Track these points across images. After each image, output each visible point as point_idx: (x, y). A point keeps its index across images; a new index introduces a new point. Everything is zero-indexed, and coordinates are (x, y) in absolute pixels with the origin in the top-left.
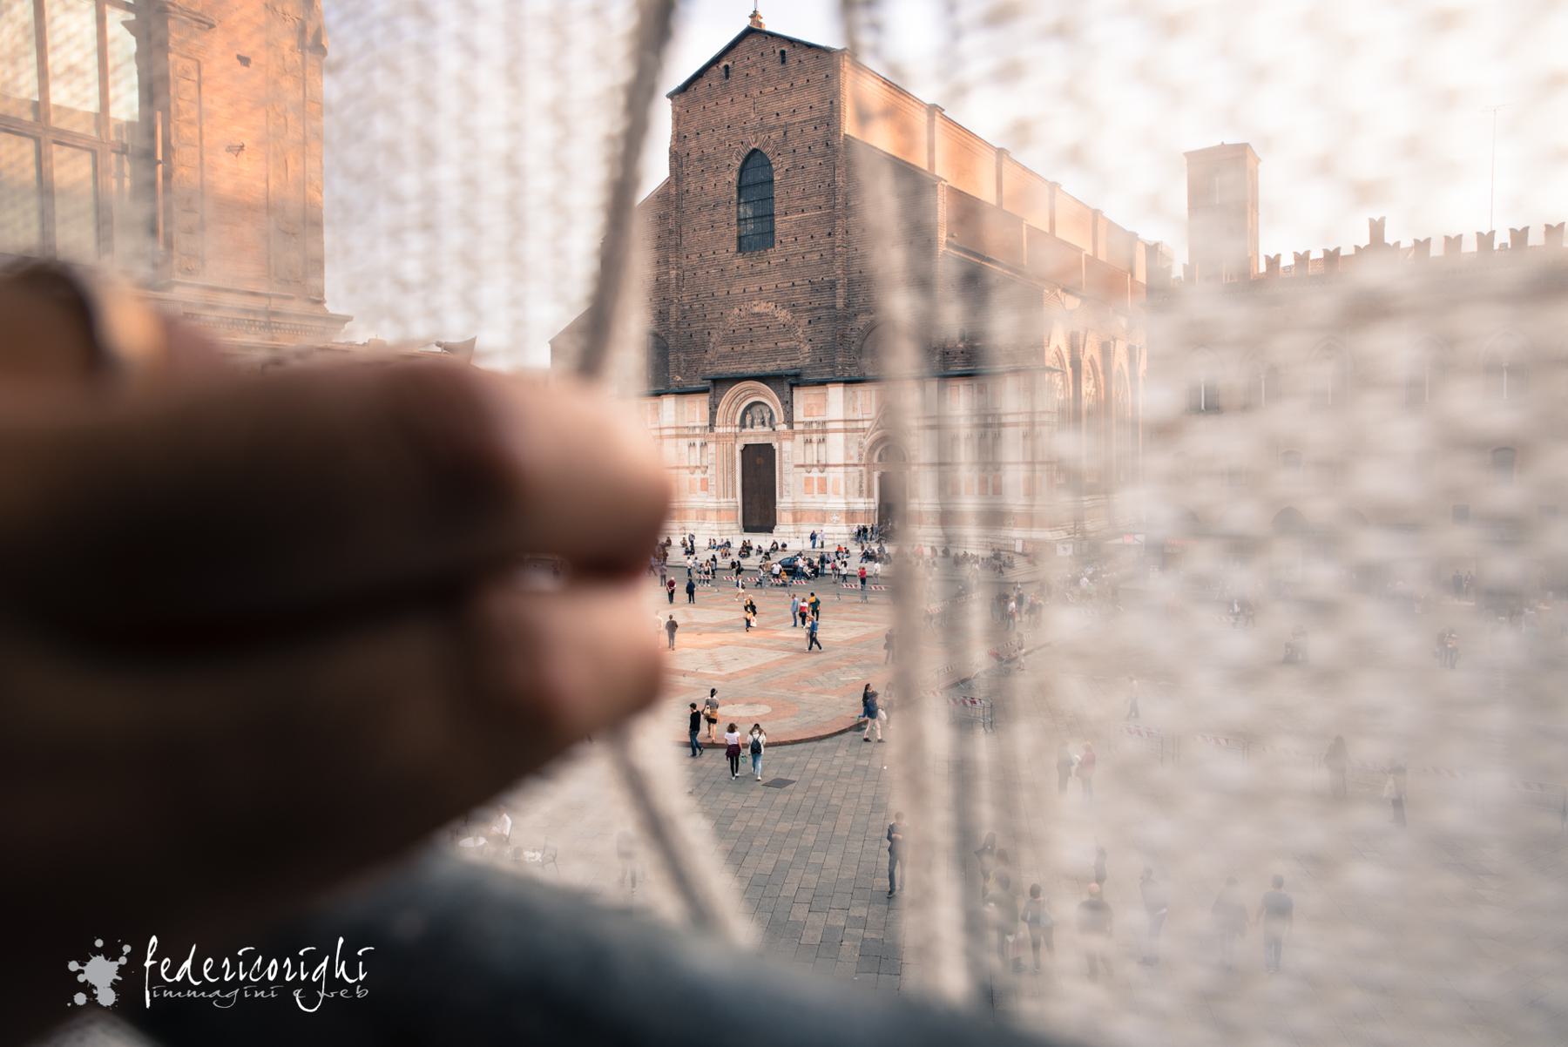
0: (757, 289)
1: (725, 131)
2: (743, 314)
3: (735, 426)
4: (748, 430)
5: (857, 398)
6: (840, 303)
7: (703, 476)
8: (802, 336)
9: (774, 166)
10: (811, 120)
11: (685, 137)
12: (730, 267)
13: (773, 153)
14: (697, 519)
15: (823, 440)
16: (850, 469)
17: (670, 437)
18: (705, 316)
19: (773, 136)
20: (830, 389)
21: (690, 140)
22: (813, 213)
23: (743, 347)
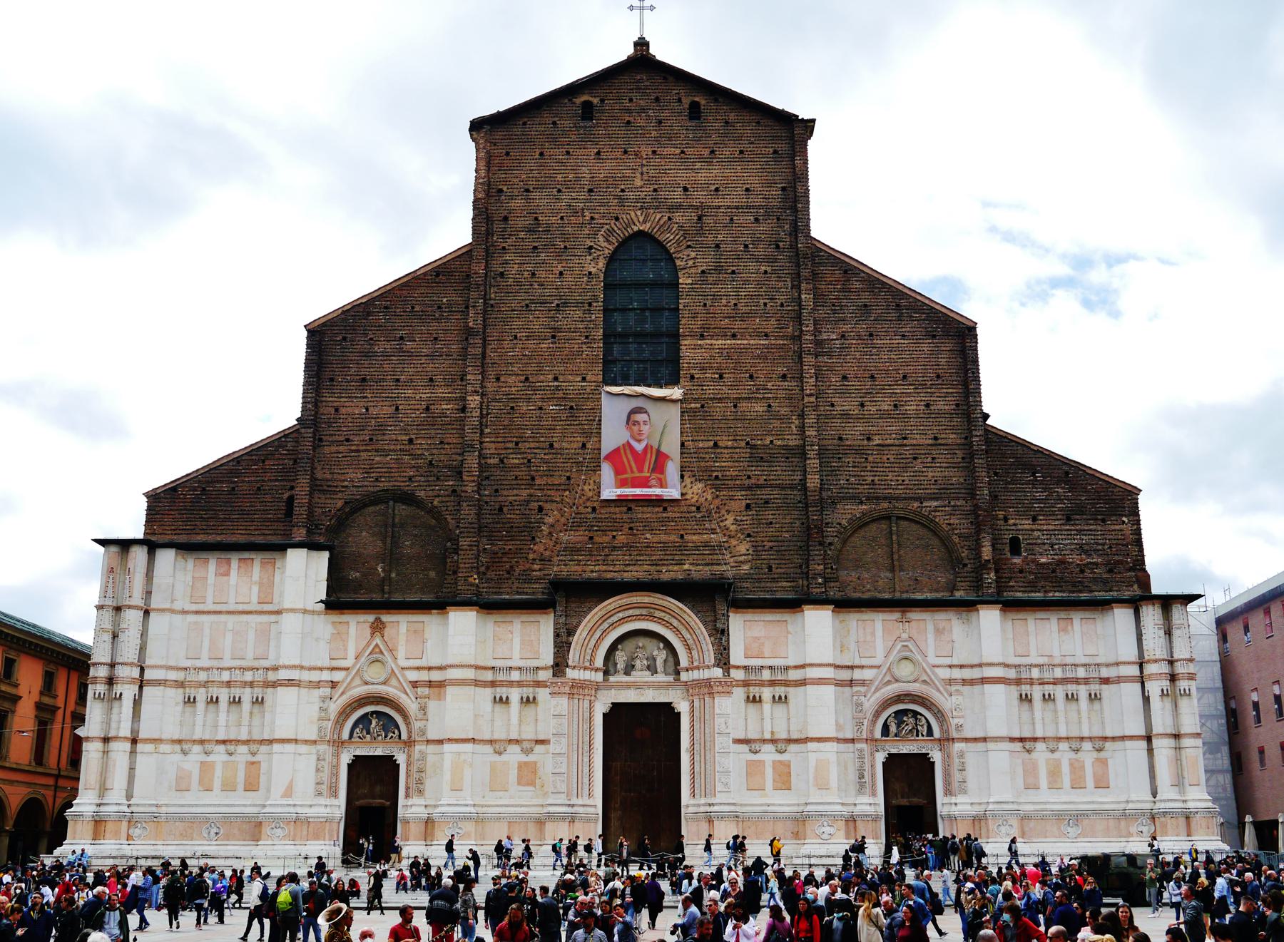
1: (584, 195)
3: (597, 670)
4: (619, 678)
5: (849, 631)
7: (523, 758)
8: (733, 528)
9: (678, 263)
10: (748, 207)
11: (501, 191)
12: (590, 405)
13: (678, 243)
15: (786, 697)
16: (842, 746)
18: (533, 479)
19: (678, 217)
21: (512, 198)
22: (752, 342)
23: (614, 537)
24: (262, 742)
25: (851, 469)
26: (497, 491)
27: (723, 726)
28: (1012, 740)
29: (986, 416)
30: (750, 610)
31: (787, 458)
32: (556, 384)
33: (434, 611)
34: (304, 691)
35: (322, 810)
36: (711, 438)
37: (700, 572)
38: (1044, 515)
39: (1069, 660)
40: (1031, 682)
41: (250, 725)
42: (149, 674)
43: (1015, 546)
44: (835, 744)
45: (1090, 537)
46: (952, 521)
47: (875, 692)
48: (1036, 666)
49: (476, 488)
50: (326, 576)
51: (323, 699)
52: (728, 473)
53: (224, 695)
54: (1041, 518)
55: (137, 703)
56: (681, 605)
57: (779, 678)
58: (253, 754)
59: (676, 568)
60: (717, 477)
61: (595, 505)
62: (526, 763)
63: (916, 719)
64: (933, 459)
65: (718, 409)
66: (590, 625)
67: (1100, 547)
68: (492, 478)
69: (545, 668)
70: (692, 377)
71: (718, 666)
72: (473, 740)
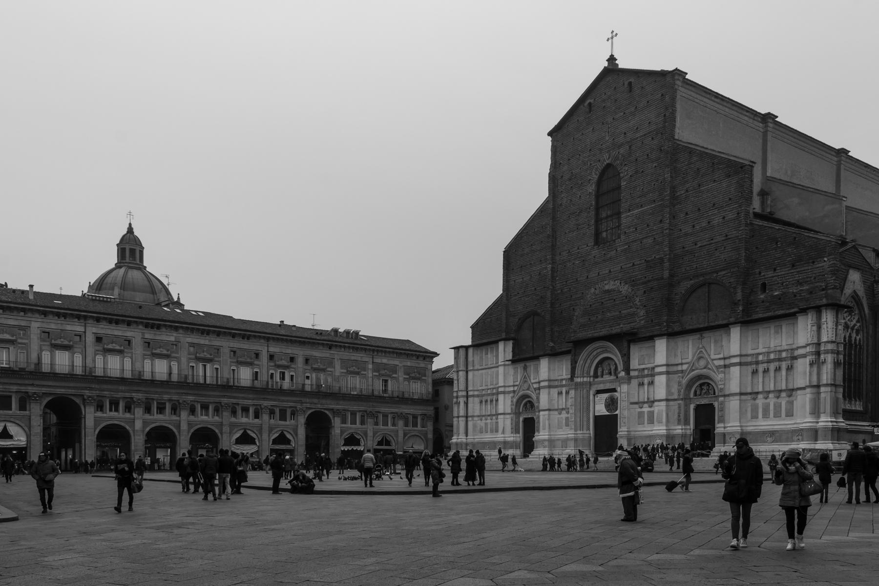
0: (607, 272)
2: (597, 292)
3: (590, 377)
4: (600, 379)
6: (666, 274)
17: (544, 387)
18: (571, 296)
20: (656, 341)
25: (687, 263)
26: (560, 304)
30: (640, 343)
31: (661, 264)
34: (507, 395)
36: (631, 261)
38: (780, 267)
41: (496, 409)
42: (470, 393)
45: (804, 274)
46: (731, 281)
50: (511, 350)
51: (512, 398)
52: (637, 277)
53: (489, 398)
54: (778, 268)
55: (466, 404)
56: (612, 345)
58: (497, 419)
59: (618, 327)
60: (633, 281)
61: (591, 303)
65: (635, 246)
66: (584, 357)
67: (809, 279)
70: (625, 233)
72: (549, 410)
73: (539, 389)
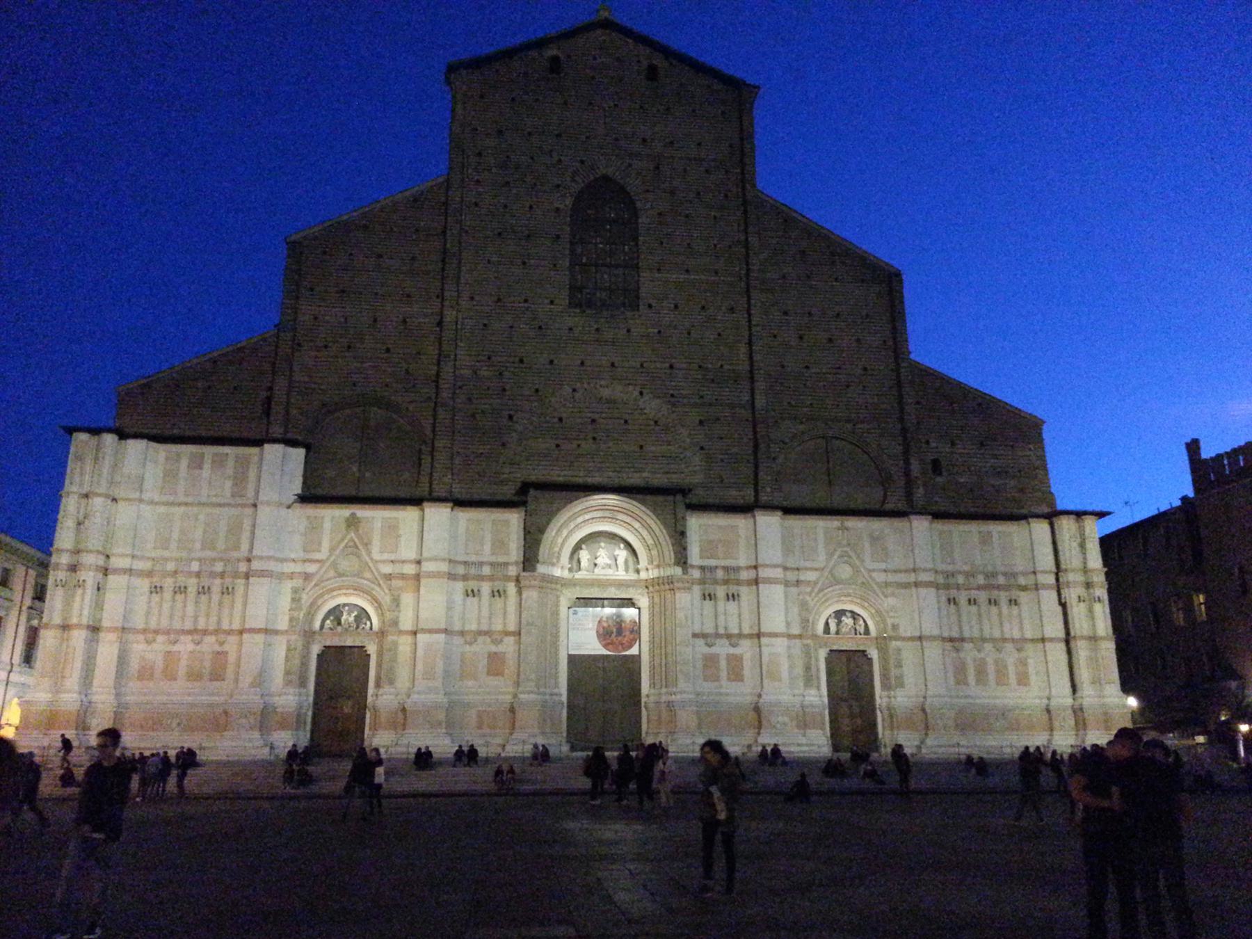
7: (494, 649)
9: (639, 204)
14: (480, 727)
23: (579, 446)
24: (229, 632)
27: (684, 622)
28: (944, 639)
29: (910, 353)
32: (526, 305)
33: (409, 508)
35: (291, 697)
37: (659, 480)
39: (990, 568)
40: (958, 587)
43: (936, 466)
44: (785, 639)
47: (818, 593)
48: (960, 572)
49: (450, 395)
51: (295, 591)
56: (643, 508)
57: (733, 577)
58: (221, 644)
60: (672, 396)
62: (495, 653)
63: (854, 619)
64: (864, 387)
68: (464, 388)
69: (516, 563)
70: (650, 306)
71: (677, 563)
72: (446, 631)
73: (417, 577)
